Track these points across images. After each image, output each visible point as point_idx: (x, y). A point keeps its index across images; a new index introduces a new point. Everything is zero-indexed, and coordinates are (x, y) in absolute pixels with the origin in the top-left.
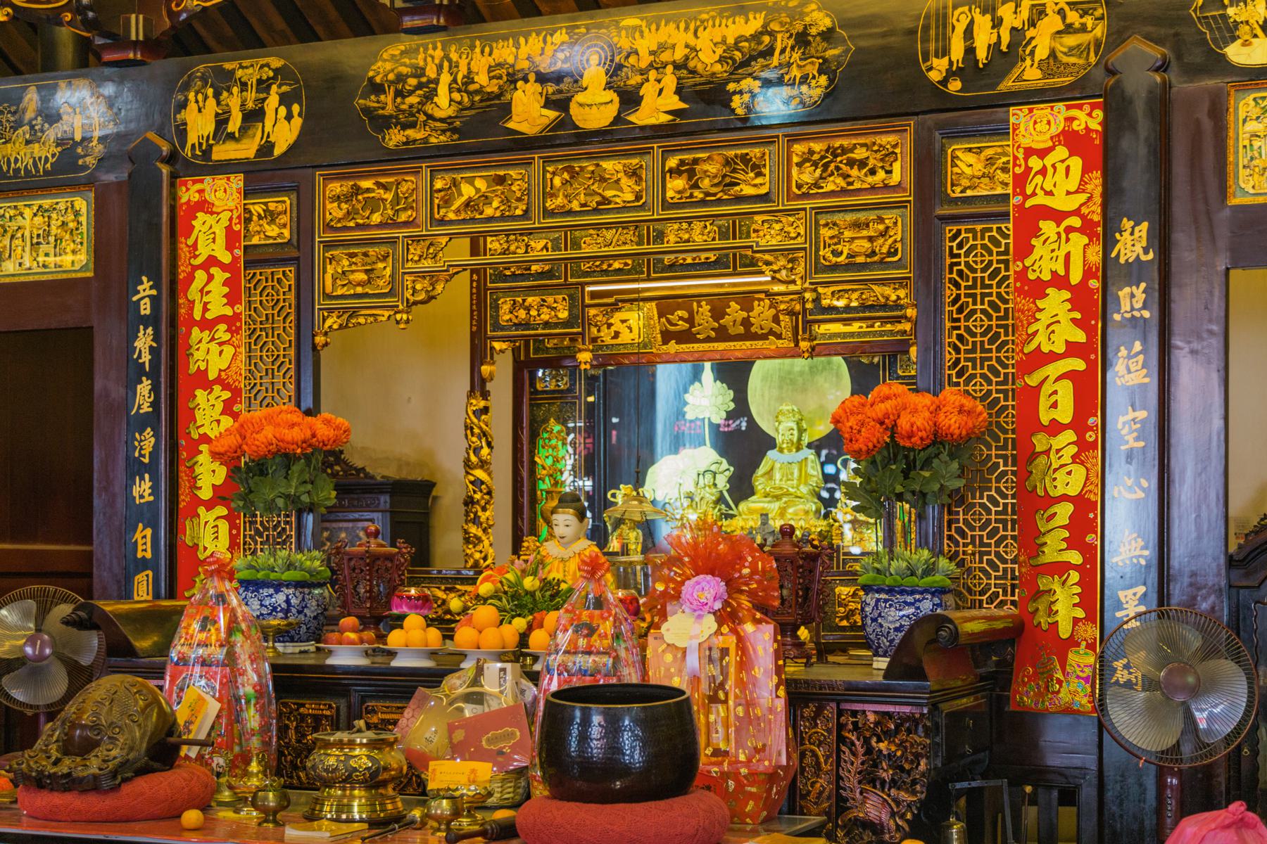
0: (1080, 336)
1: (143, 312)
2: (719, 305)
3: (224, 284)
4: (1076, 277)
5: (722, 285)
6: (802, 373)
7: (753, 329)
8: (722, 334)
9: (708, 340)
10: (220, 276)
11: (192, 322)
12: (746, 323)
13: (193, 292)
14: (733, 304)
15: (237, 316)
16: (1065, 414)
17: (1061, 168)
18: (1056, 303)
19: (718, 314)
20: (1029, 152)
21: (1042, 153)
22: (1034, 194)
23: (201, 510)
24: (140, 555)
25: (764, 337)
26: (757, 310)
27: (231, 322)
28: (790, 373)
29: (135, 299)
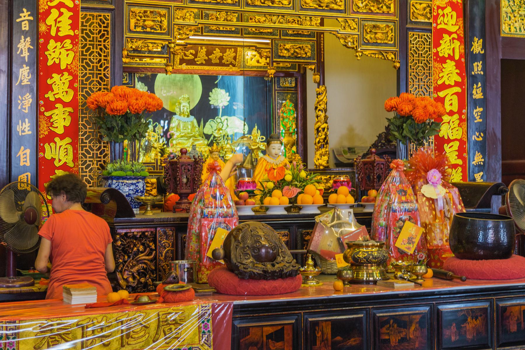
0: (459, 79)
1: (23, 29)
2: (210, 48)
3: (70, 18)
4: (457, 57)
5: (203, 40)
6: (179, 81)
7: (223, 61)
8: (208, 62)
9: (202, 64)
10: (67, 14)
11: (48, 37)
12: (221, 58)
13: (50, 21)
14: (217, 49)
15: (76, 36)
16: (455, 108)
17: (450, 15)
18: (450, 66)
19: (209, 53)
20: (439, 7)
21: (443, 9)
22: (441, 23)
23: (57, 139)
24: (22, 164)
25: (228, 65)
26: (228, 52)
27: (73, 39)
28: (174, 80)
29: (18, 20)
